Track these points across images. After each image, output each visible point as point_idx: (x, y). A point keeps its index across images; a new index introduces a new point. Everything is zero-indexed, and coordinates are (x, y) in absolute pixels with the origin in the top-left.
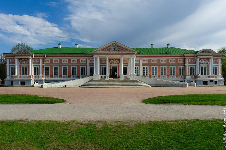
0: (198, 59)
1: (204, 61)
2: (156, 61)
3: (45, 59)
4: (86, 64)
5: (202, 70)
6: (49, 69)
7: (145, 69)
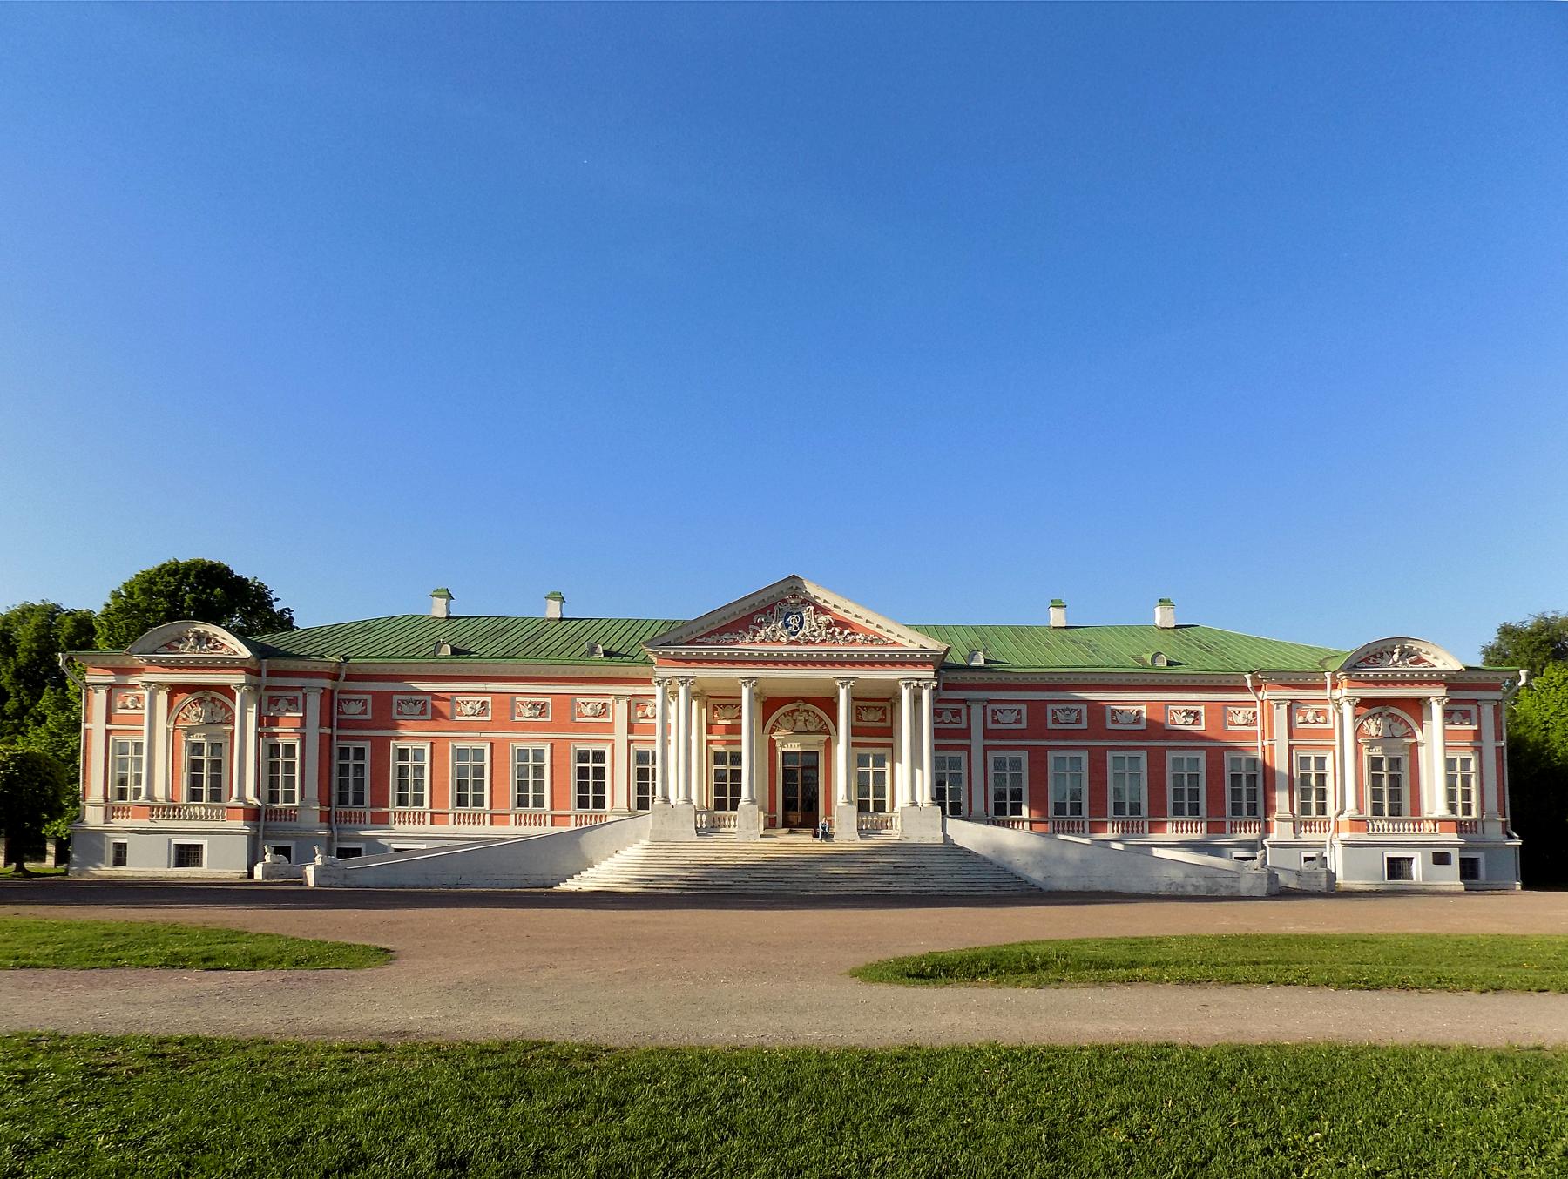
2: (1074, 716)
3: (340, 692)
4: (611, 731)
5: (1376, 780)
6: (367, 762)
7: (1008, 772)
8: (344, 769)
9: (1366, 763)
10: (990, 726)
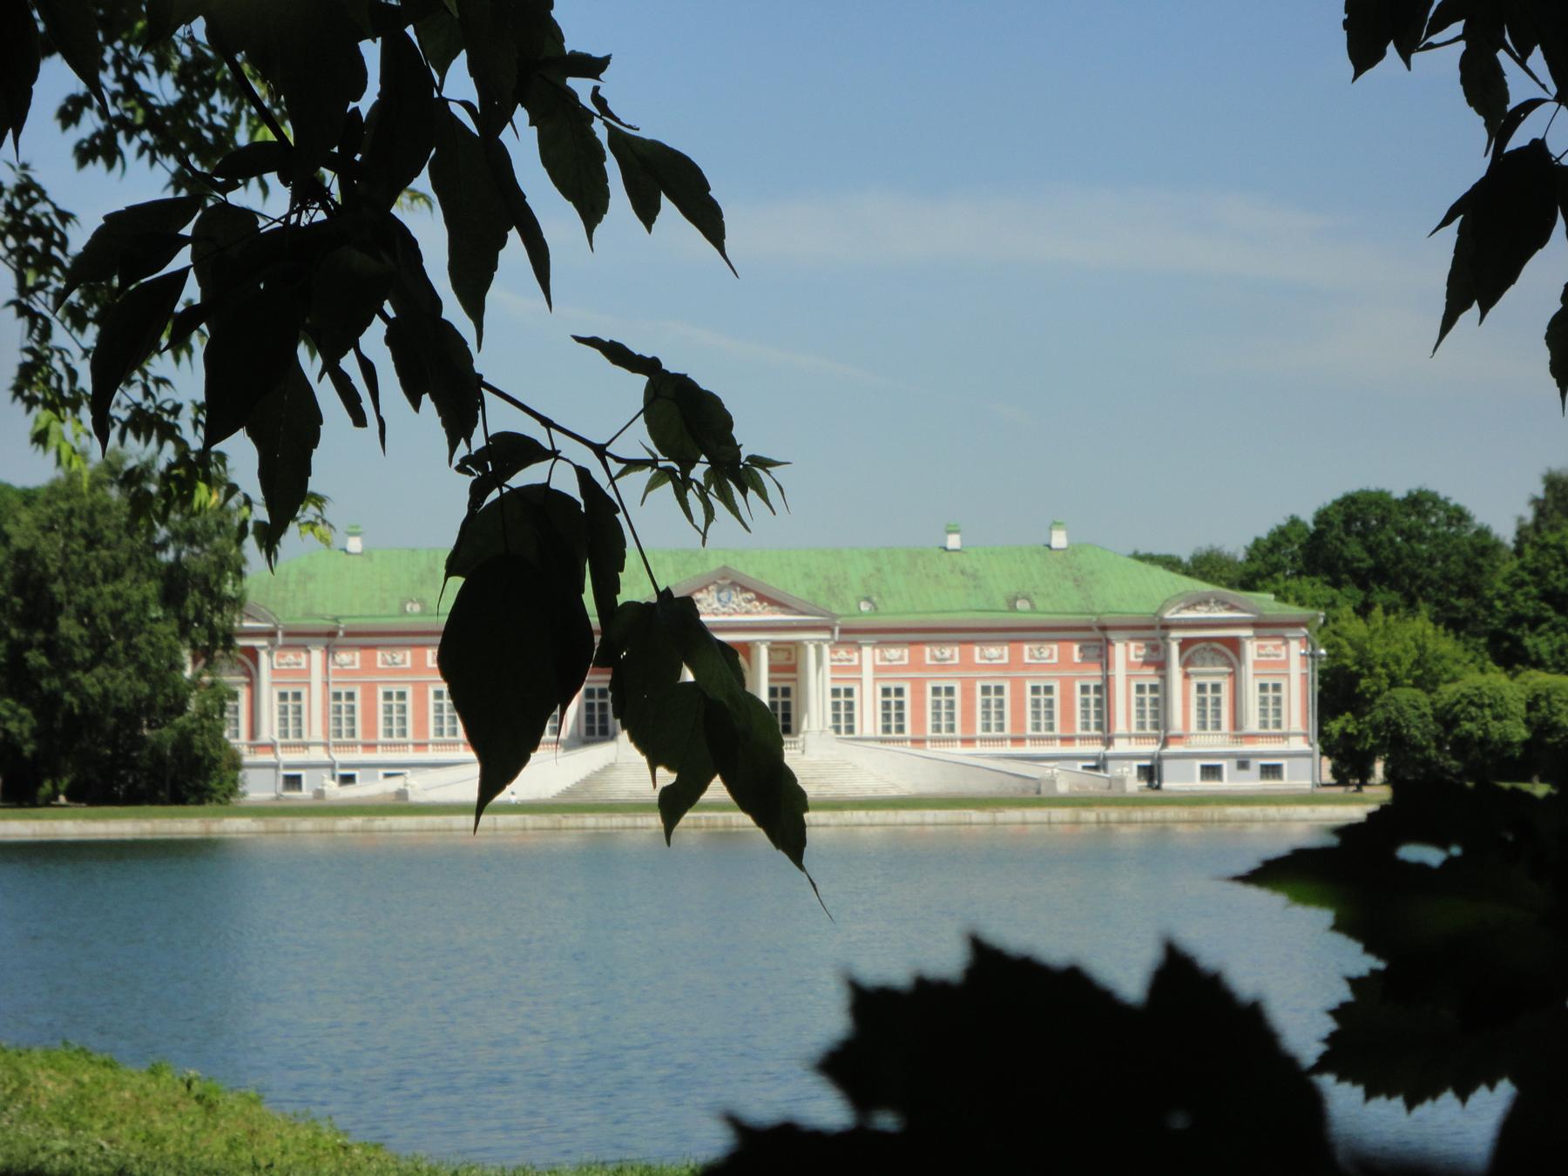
0: (1175, 649)
1: (1208, 655)
5: (1202, 702)
8: (338, 710)
9: (1194, 688)
10: (878, 662)
